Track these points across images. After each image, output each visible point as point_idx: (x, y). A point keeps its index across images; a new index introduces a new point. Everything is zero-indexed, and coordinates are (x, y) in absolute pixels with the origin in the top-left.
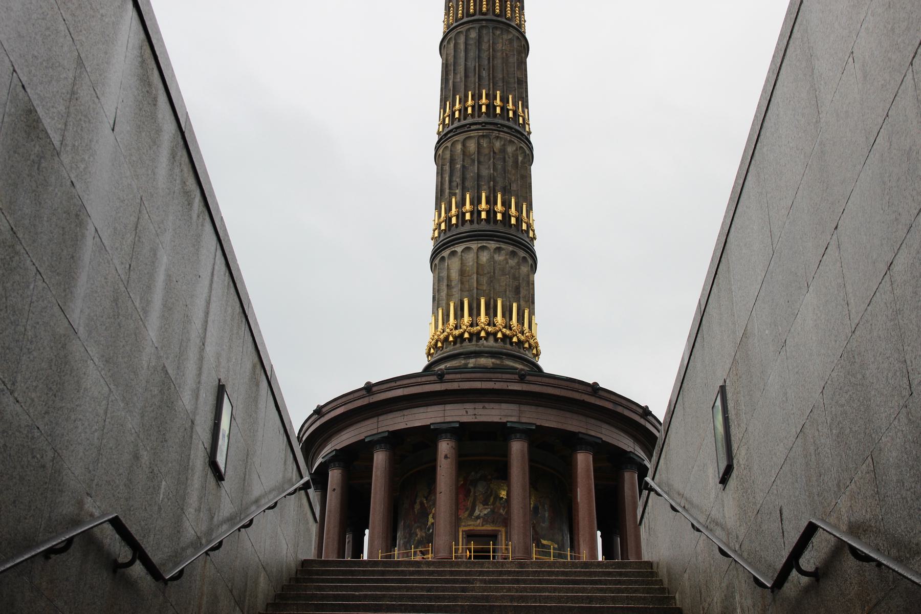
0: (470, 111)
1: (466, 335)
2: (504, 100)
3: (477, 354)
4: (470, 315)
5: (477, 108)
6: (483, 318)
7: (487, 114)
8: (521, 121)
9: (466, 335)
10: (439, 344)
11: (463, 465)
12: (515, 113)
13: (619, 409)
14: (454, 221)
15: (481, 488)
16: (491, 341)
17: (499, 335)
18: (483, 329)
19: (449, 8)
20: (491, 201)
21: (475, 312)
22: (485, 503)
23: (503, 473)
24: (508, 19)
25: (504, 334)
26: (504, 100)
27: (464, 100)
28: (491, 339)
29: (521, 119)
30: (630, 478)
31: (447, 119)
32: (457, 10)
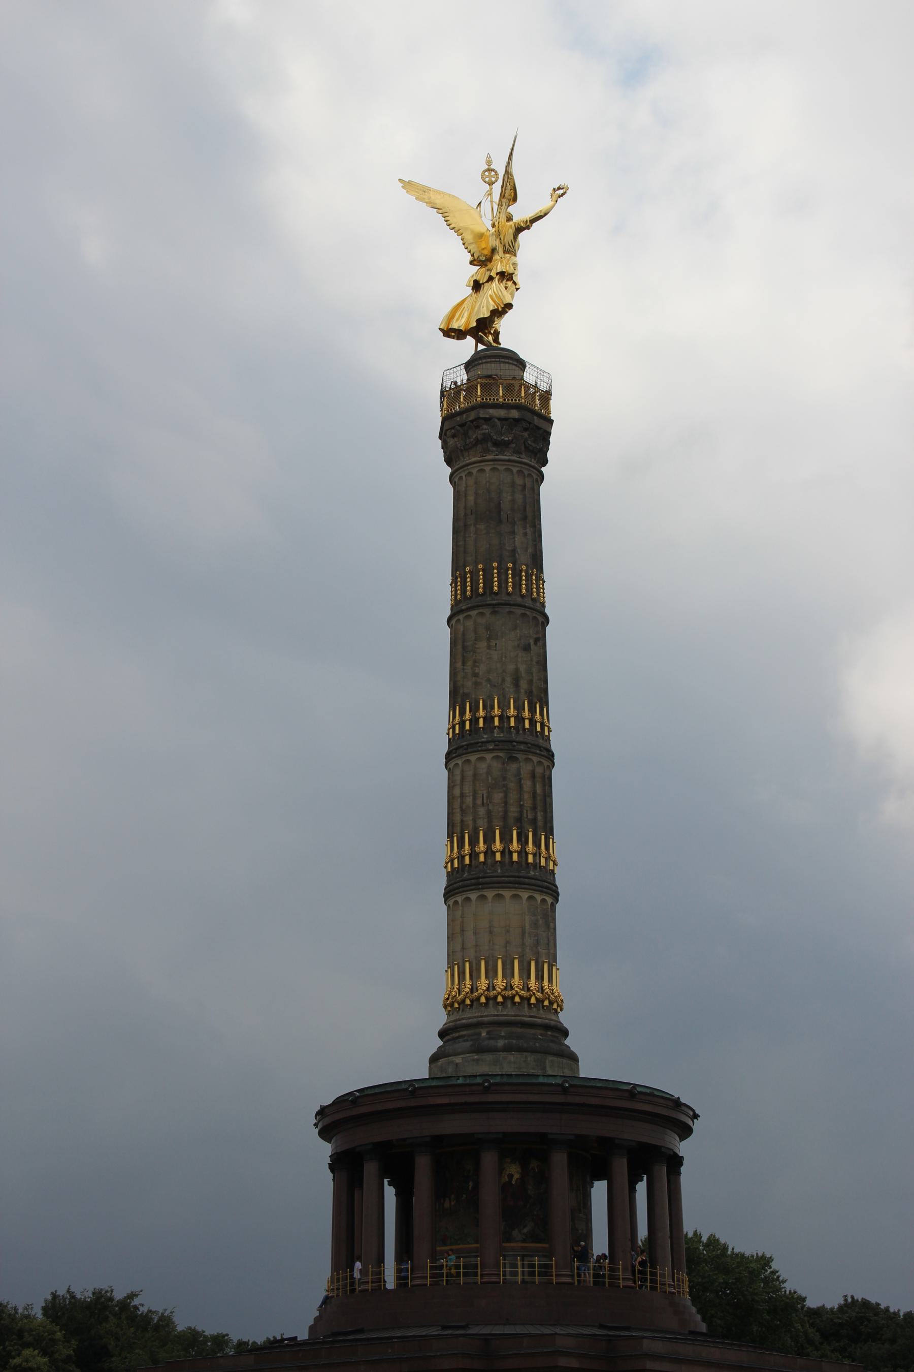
0: (481, 724)
1: (483, 1000)
4: (487, 977)
8: (539, 729)
9: (483, 1000)
10: (456, 1005)
12: (533, 722)
18: (499, 994)
19: (457, 578)
20: (506, 839)
21: (491, 974)
24: (523, 596)
25: (521, 997)
28: (509, 1003)
29: (538, 725)
31: (457, 727)
32: (466, 582)
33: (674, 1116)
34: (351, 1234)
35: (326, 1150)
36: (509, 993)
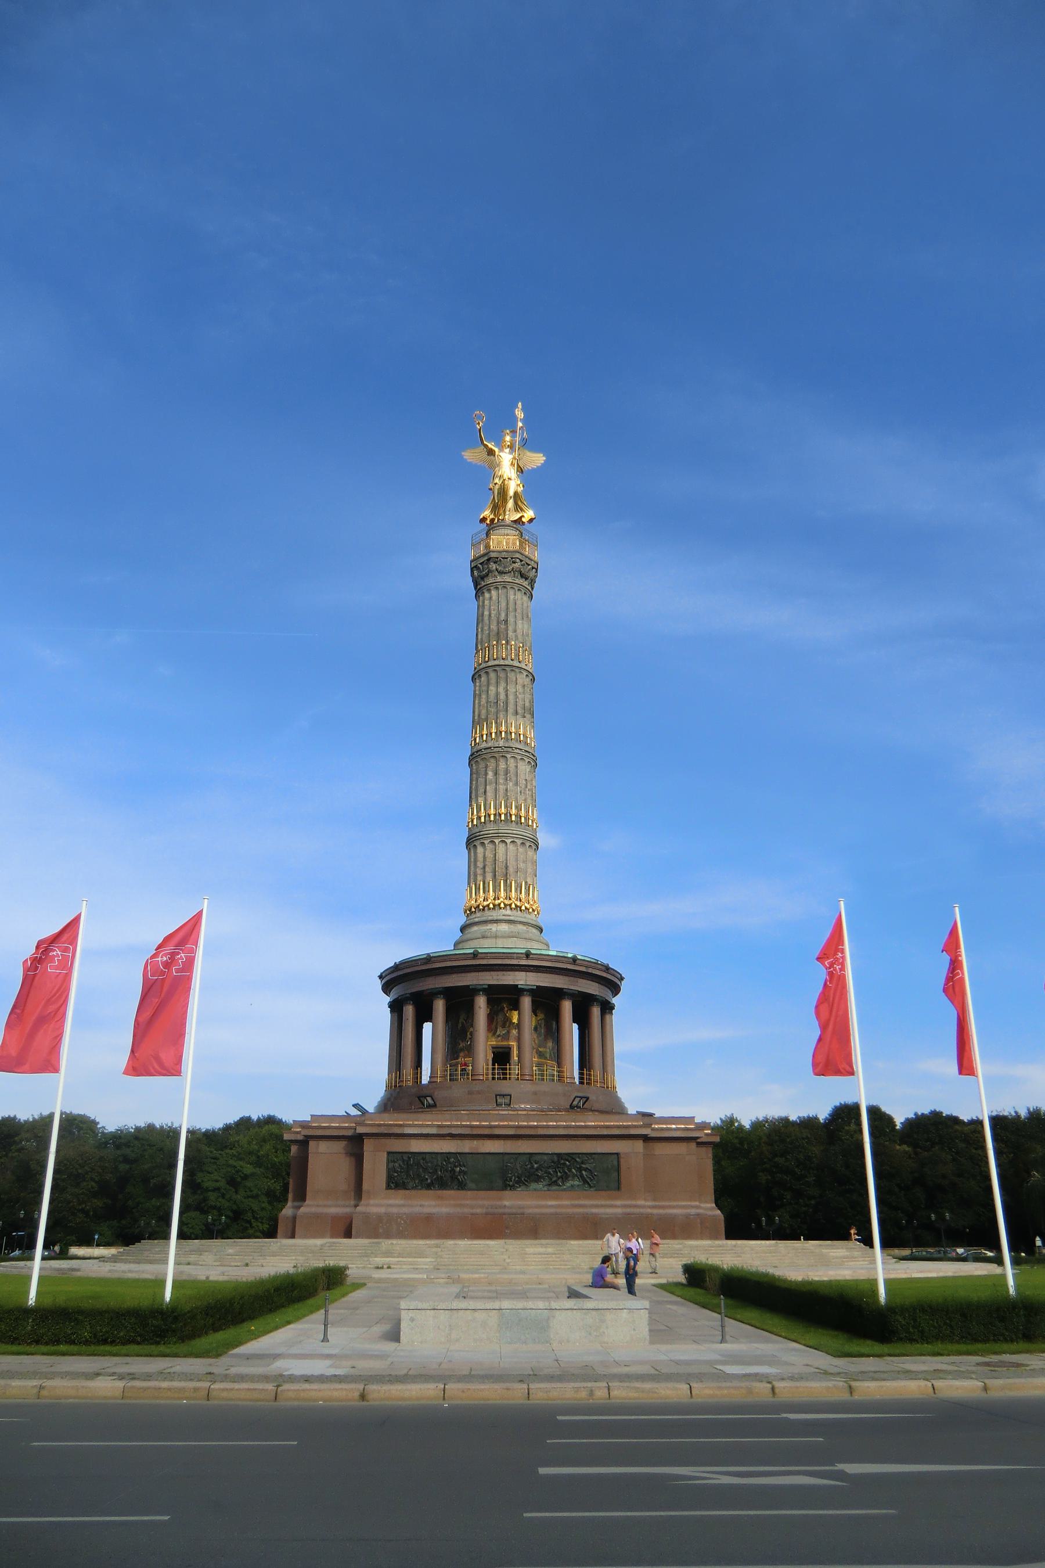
1: (491, 906)
2: (518, 727)
3: (497, 921)
4: (494, 891)
5: (499, 733)
6: (502, 894)
7: (506, 739)
11: (489, 1002)
13: (590, 970)
14: (483, 820)
15: (500, 1017)
16: (508, 912)
17: (513, 906)
22: (503, 1026)
23: (516, 1006)
25: (516, 906)
26: (518, 727)
27: (489, 727)
30: (596, 1011)
33: (611, 981)
34: (403, 1052)
35: (387, 999)
36: (507, 902)
